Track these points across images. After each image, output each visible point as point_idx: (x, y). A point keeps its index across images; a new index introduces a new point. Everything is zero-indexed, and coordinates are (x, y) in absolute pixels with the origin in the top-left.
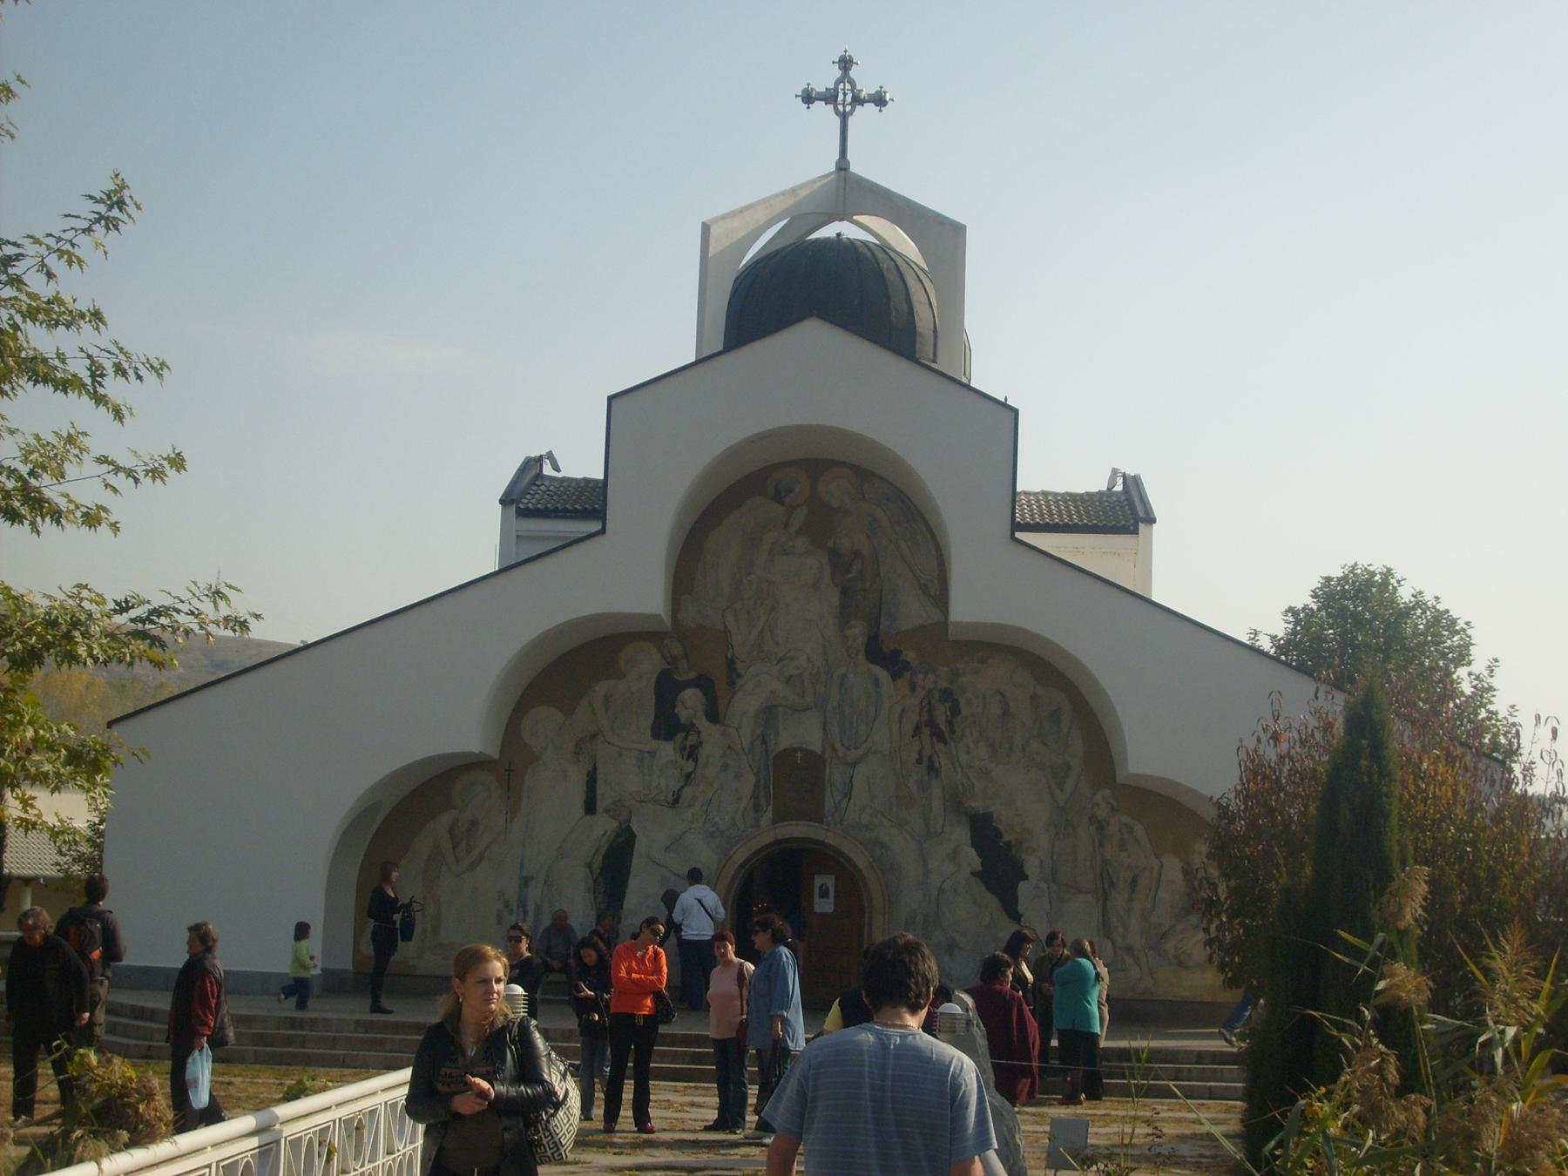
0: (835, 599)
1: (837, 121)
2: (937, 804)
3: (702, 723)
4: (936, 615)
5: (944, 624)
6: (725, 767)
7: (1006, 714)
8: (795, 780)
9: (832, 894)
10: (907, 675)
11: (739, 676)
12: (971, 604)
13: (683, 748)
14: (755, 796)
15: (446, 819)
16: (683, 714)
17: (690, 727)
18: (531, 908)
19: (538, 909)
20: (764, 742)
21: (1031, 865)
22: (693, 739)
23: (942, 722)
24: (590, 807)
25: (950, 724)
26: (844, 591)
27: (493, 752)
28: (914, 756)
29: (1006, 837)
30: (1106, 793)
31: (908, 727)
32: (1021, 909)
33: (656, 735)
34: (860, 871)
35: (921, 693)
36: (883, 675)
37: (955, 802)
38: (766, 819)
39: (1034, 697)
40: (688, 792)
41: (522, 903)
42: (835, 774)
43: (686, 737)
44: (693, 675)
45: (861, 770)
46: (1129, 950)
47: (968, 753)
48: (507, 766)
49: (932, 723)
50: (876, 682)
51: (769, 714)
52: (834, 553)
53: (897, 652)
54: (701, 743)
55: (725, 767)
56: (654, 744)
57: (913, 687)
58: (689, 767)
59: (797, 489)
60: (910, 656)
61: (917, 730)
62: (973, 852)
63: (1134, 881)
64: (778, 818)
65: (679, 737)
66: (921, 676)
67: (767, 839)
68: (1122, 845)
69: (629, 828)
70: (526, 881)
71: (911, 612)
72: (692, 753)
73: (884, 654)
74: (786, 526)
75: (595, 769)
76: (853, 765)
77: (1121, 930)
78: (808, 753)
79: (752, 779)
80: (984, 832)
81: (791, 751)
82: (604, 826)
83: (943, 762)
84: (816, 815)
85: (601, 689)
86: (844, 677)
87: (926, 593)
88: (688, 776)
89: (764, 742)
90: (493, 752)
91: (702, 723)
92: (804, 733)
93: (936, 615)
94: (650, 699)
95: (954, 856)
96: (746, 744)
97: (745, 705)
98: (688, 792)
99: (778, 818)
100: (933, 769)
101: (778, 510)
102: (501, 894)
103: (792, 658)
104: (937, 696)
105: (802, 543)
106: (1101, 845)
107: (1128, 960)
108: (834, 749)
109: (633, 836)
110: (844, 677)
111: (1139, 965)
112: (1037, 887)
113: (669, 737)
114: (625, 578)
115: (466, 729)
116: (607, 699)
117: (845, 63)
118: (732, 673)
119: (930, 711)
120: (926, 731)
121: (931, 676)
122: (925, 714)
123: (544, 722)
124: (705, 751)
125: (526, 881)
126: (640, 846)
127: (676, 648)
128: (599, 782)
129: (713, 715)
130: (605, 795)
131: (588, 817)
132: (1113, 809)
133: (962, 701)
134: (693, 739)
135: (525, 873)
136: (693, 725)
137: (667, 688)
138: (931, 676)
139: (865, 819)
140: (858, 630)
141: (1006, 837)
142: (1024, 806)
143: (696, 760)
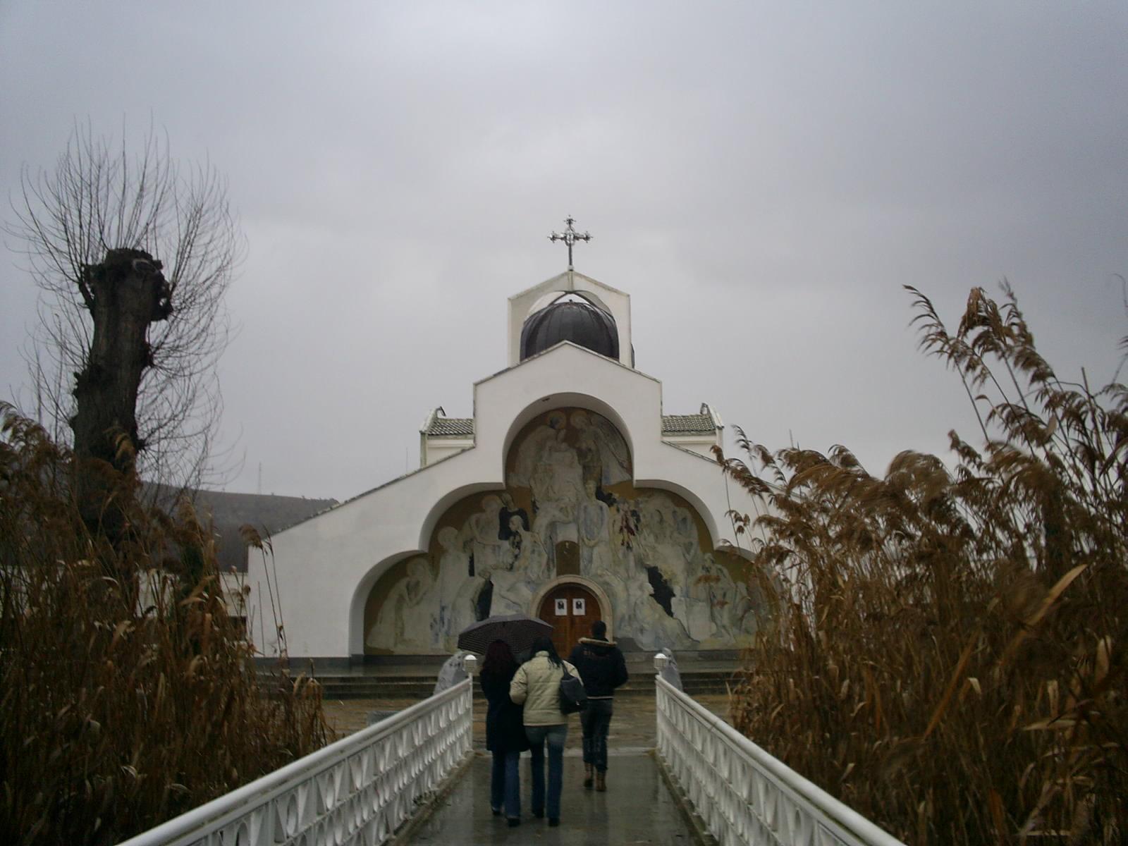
1: (568, 247)
2: (632, 563)
3: (521, 531)
4: (627, 477)
6: (533, 552)
7: (661, 521)
8: (567, 557)
9: (583, 605)
10: (615, 505)
11: (538, 508)
12: (643, 471)
13: (513, 543)
14: (548, 564)
15: (404, 581)
16: (513, 527)
18: (446, 621)
19: (449, 621)
21: (677, 590)
22: (518, 538)
23: (633, 528)
24: (472, 573)
25: (636, 526)
26: (584, 467)
27: (426, 550)
28: (621, 542)
32: (673, 610)
33: (500, 538)
34: (596, 595)
36: (604, 505)
37: (640, 563)
40: (516, 564)
41: (442, 619)
42: (584, 552)
44: (516, 509)
45: (596, 551)
46: (724, 627)
47: (645, 539)
48: (432, 553)
49: (628, 527)
50: (601, 508)
51: (553, 526)
54: (521, 541)
55: (533, 552)
56: (500, 542)
57: (618, 510)
58: (517, 551)
60: (616, 496)
61: (621, 529)
64: (559, 574)
65: (512, 538)
67: (555, 583)
69: (490, 582)
70: (443, 609)
71: (615, 475)
72: (517, 545)
74: (556, 439)
75: (473, 555)
76: (592, 547)
77: (719, 617)
78: (572, 544)
79: (546, 556)
81: (563, 543)
82: (479, 581)
83: (633, 544)
84: (575, 570)
85: (474, 518)
86: (586, 507)
87: (623, 467)
90: (426, 550)
91: (521, 531)
92: (569, 534)
93: (627, 477)
94: (497, 522)
95: (641, 588)
97: (541, 522)
98: (516, 564)
99: (559, 574)
100: (629, 547)
101: (551, 432)
102: (432, 615)
104: (629, 513)
105: (564, 446)
107: (723, 630)
108: (583, 540)
109: (492, 585)
111: (729, 634)
112: (680, 600)
113: (507, 538)
114: (484, 466)
115: (412, 541)
116: (477, 522)
118: (535, 508)
120: (625, 530)
121: (626, 504)
122: (624, 523)
123: (449, 534)
125: (443, 609)
126: (496, 589)
127: (507, 497)
128: (476, 560)
130: (478, 567)
131: (473, 578)
133: (641, 515)
135: (443, 605)
137: (505, 516)
138: (626, 504)
139: (599, 572)
140: (592, 486)
142: (673, 564)
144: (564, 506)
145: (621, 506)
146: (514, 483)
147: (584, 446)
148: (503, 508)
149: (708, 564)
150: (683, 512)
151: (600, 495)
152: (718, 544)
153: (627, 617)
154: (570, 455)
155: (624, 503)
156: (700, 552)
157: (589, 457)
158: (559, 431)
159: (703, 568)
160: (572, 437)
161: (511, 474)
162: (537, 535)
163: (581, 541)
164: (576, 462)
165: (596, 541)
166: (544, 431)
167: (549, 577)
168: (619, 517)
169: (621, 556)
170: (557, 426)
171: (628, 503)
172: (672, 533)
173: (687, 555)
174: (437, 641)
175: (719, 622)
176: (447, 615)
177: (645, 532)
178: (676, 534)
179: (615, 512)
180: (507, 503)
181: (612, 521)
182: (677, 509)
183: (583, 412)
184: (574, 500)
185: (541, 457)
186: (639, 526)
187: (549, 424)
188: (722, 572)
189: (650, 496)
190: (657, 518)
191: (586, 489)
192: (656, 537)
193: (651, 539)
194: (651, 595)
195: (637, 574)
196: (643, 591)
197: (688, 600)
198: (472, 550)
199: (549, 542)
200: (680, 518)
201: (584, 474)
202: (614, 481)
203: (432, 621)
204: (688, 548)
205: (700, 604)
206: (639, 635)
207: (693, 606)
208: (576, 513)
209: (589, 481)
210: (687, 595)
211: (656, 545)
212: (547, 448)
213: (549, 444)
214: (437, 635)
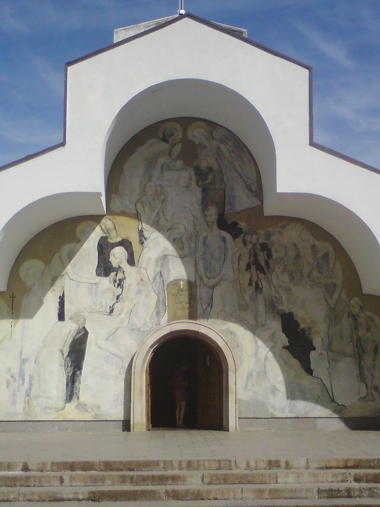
0: (200, 196)
2: (261, 308)
3: (125, 266)
4: (256, 202)
5: (261, 208)
6: (139, 292)
7: (298, 257)
11: (145, 239)
14: (157, 306)
17: (119, 269)
18: (27, 377)
19: (31, 378)
20: (161, 276)
21: (317, 342)
22: (120, 276)
23: (263, 264)
24: (61, 317)
25: (267, 263)
26: (204, 190)
28: (247, 281)
29: (302, 326)
30: (356, 299)
31: (243, 264)
32: (312, 367)
33: (98, 274)
35: (250, 246)
36: (228, 236)
37: (271, 306)
38: (165, 318)
39: (313, 247)
43: (116, 275)
44: (119, 239)
45: (217, 292)
47: (278, 278)
50: (224, 240)
52: (197, 170)
53: (235, 224)
54: (125, 278)
55: (139, 292)
56: (98, 279)
57: (245, 243)
59: (176, 133)
60: (243, 225)
61: (248, 267)
62: (283, 335)
63: (376, 348)
65: (113, 274)
66: (249, 236)
68: (368, 329)
69: (84, 328)
70: (24, 361)
71: (243, 201)
72: (120, 284)
74: (170, 155)
75: (63, 295)
76: (213, 287)
79: (155, 298)
80: (289, 324)
83: (264, 284)
87: (250, 190)
88: (118, 297)
89: (161, 276)
93: (256, 202)
94: (95, 254)
96: (151, 277)
100: (258, 289)
101: (164, 146)
102: (9, 370)
103: (176, 228)
104: (259, 247)
105: (179, 163)
106: (356, 328)
108: (201, 279)
109: (86, 334)
110: (205, 238)
113: (107, 275)
119: (256, 255)
120: (253, 268)
121: (255, 236)
122: (252, 259)
124: (126, 284)
125: (24, 361)
129: (131, 261)
132: (361, 308)
133: (273, 250)
134: (120, 276)
135: (23, 357)
136: (120, 267)
137: (104, 248)
140: (213, 212)
141: (302, 326)
143: (122, 288)
144: (178, 236)
145: (248, 238)
147: (204, 165)
148: (102, 238)
149: (356, 310)
150: (324, 246)
151: (223, 223)
152: (366, 290)
153: (255, 374)
154: (186, 175)
155: (252, 234)
156: (344, 296)
157: (210, 177)
158: (173, 146)
159: (349, 314)
160: (189, 153)
161: (113, 196)
162: (144, 271)
163: (198, 279)
164: (194, 183)
165: (217, 280)
166: (155, 146)
167: (158, 324)
168: (245, 251)
169: (247, 298)
170: (170, 141)
171: (256, 234)
172: (311, 272)
173: (329, 300)
174: (14, 402)
175: (370, 384)
176: (29, 369)
177: (278, 271)
178: (315, 274)
179: (241, 245)
180: (108, 231)
181: (237, 255)
182: (317, 243)
183: (202, 124)
184: (190, 228)
185: (151, 176)
186: (270, 262)
187: (161, 136)
188: (372, 319)
189: (283, 227)
190: (292, 254)
191: (205, 216)
192: (292, 277)
193: (286, 278)
194: (285, 347)
195: (268, 322)
196: (276, 343)
197: (330, 353)
198: (63, 288)
199: (158, 279)
200: (320, 255)
201: (203, 198)
202: (239, 208)
203: (8, 377)
204: (330, 289)
205: (347, 359)
206: (271, 397)
207: (336, 361)
208: (193, 245)
209: (210, 207)
210: (329, 348)
211: (291, 286)
212: (159, 167)
213: (161, 161)
214: (14, 394)
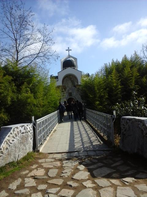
42: (72, 93)
51: (68, 90)
71: (76, 84)
73: (74, 86)
81: (69, 93)
84: (71, 96)
92: (70, 91)
97: (67, 90)
101: (67, 78)
105: (69, 80)
117: (69, 48)
118: (66, 88)
140: (73, 85)
146: (63, 85)
151: (74, 86)
154: (70, 81)
160: (70, 79)
